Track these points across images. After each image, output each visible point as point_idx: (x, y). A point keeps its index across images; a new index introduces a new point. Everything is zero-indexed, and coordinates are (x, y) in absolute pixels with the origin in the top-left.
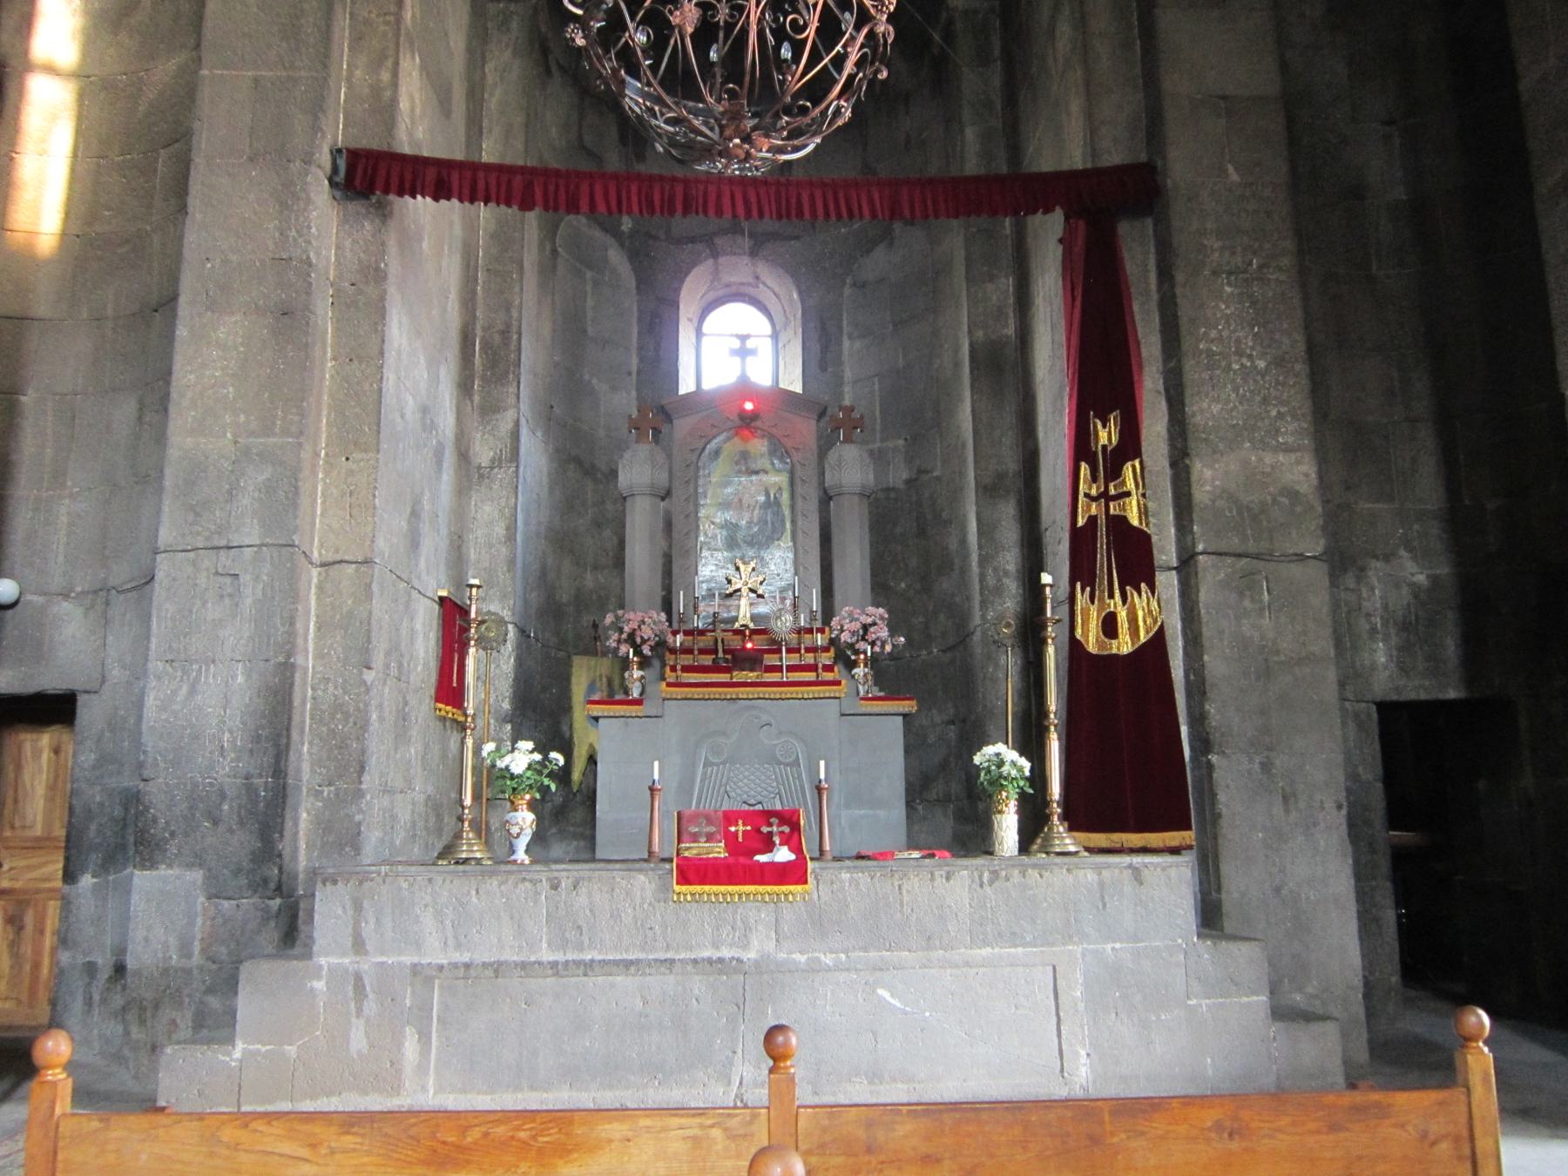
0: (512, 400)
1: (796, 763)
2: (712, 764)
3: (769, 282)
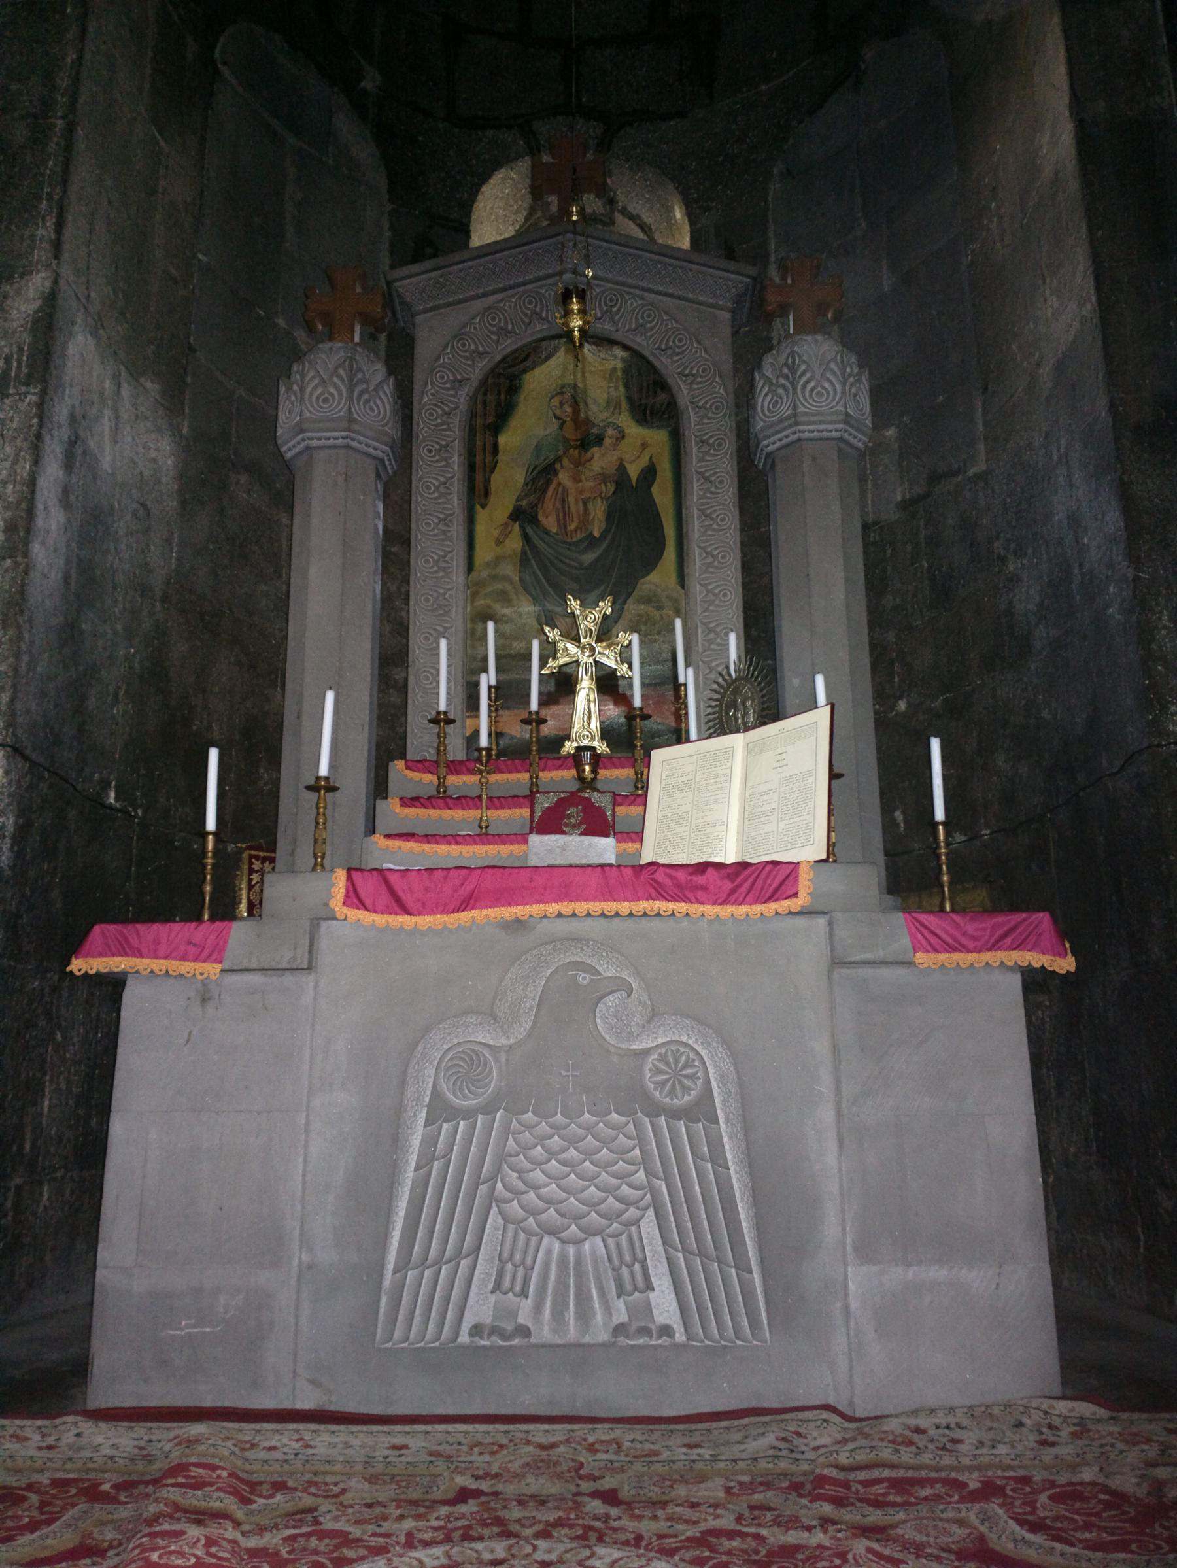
0: (41, 253)
1: (702, 1110)
2: (454, 1114)
3: (635, 207)
